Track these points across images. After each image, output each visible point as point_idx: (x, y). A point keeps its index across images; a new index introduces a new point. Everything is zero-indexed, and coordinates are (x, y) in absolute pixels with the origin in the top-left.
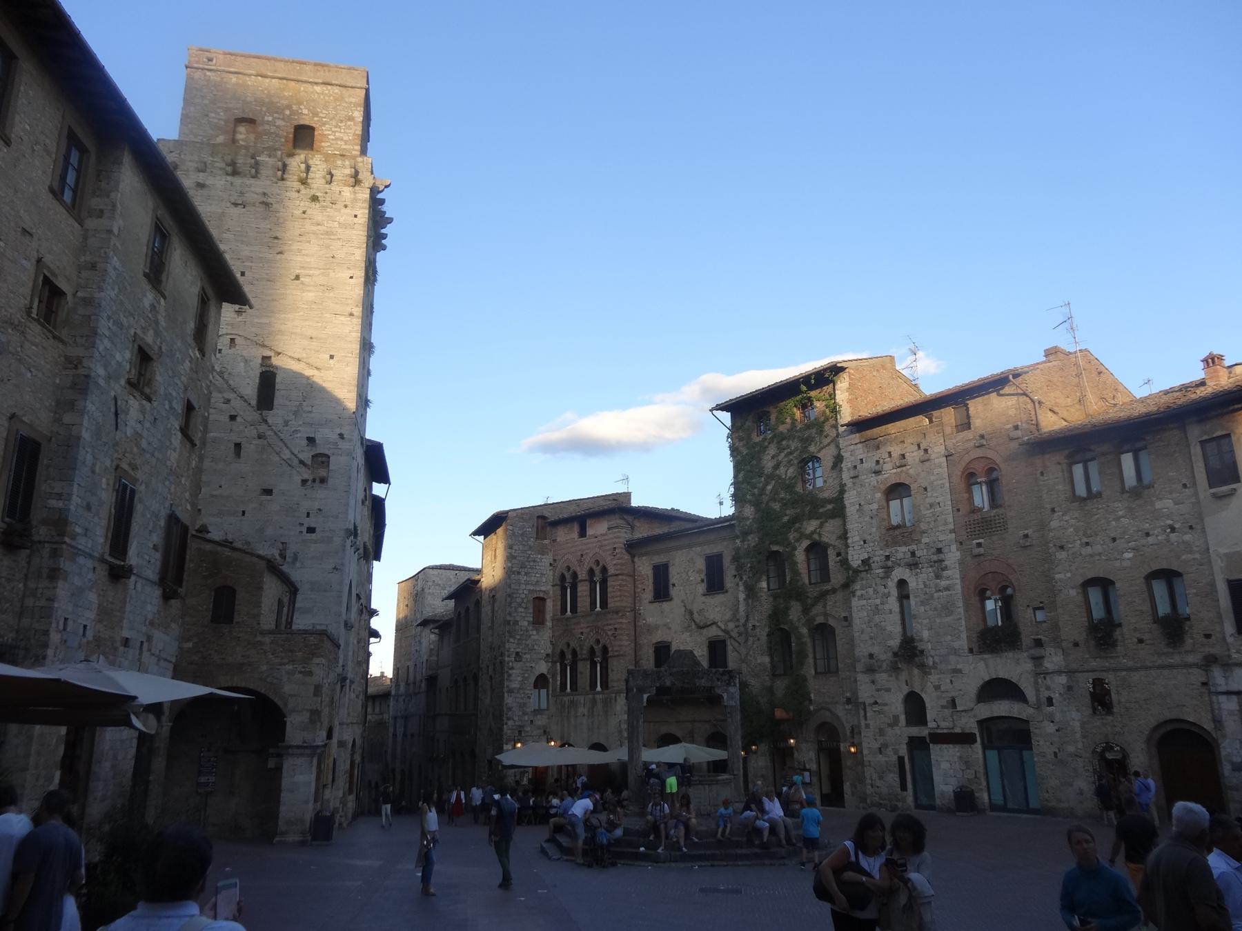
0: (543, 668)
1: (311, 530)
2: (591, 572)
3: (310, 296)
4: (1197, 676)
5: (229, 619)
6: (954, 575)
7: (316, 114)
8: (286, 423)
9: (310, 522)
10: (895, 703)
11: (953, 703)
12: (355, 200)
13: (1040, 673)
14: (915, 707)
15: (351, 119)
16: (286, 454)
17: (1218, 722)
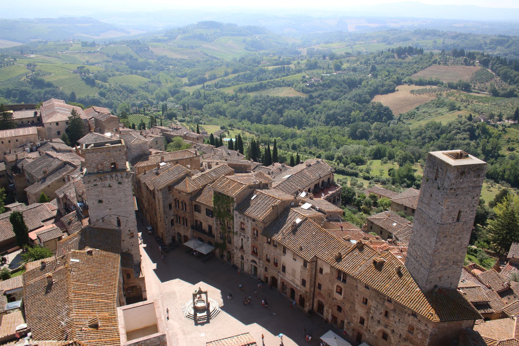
0: (172, 218)
1: (133, 245)
2: (182, 202)
3: (123, 204)
4: (277, 273)
5: (130, 277)
6: (250, 242)
7: (115, 160)
8: (124, 228)
9: (132, 244)
10: (240, 255)
11: (248, 260)
12: (128, 181)
13: (259, 262)
14: (242, 258)
15: (123, 159)
16: (125, 234)
17: (278, 278)
